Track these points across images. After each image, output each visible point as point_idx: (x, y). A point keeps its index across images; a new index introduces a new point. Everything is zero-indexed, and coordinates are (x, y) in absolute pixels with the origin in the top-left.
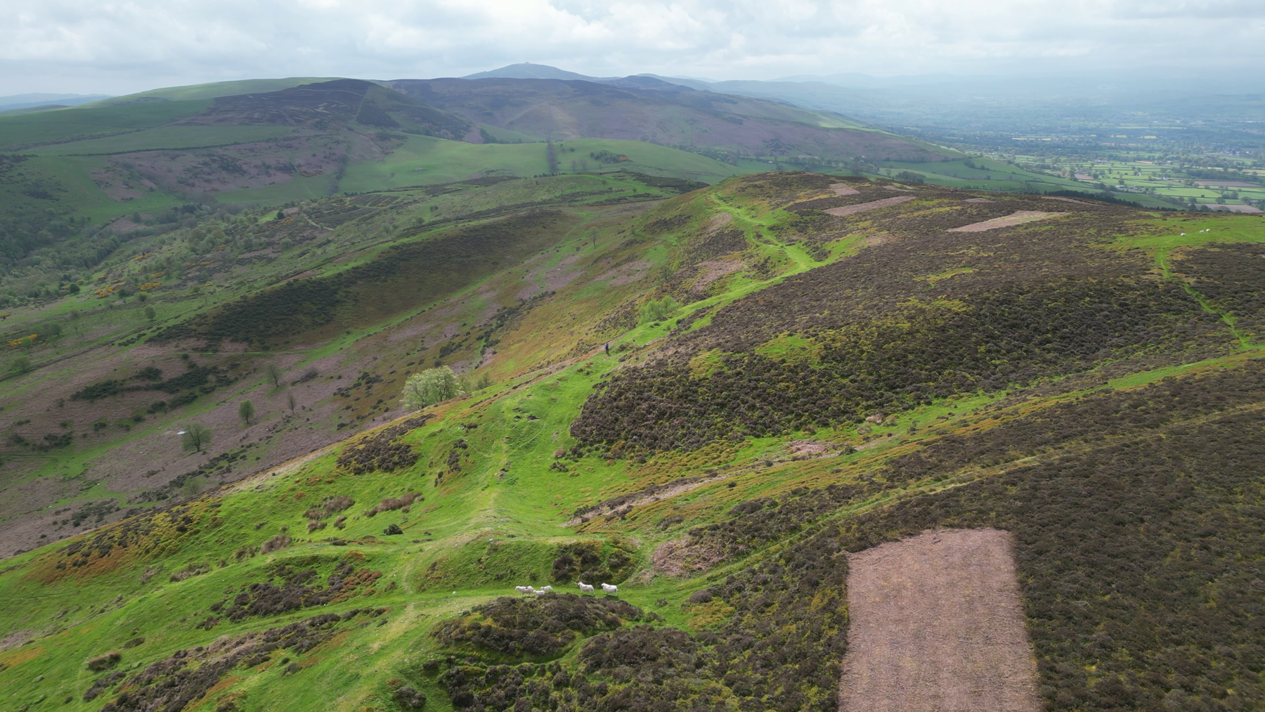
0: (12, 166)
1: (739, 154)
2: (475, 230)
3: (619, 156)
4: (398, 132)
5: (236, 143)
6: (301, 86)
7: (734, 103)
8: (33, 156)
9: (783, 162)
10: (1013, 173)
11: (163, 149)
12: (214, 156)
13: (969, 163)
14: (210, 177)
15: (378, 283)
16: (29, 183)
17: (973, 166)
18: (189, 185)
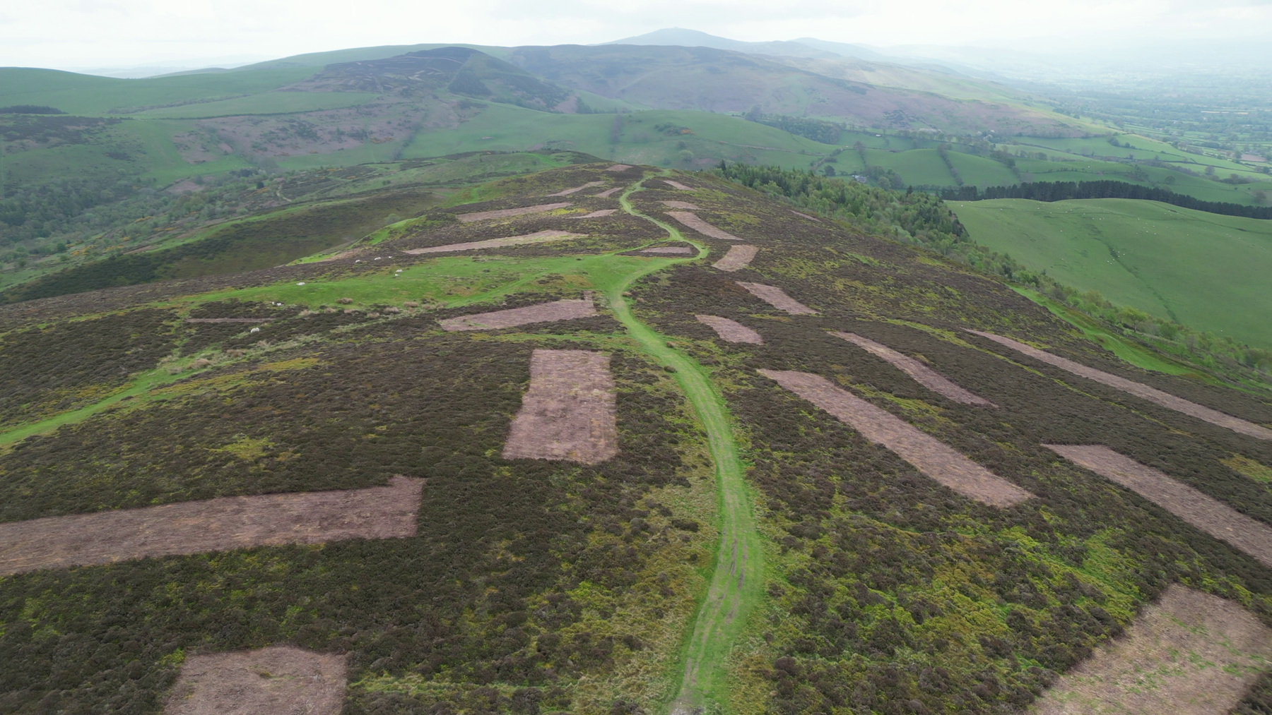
0: (104, 128)
1: (845, 125)
2: (324, 210)
3: (683, 128)
4: (486, 101)
5: (320, 110)
6: (408, 54)
7: (871, 70)
8: (129, 119)
9: (891, 135)
10: (1163, 152)
11: (251, 115)
12: (294, 121)
13: (1113, 141)
14: (283, 142)
15: (203, 260)
16: (114, 144)
17: (1116, 144)
18: (261, 149)
